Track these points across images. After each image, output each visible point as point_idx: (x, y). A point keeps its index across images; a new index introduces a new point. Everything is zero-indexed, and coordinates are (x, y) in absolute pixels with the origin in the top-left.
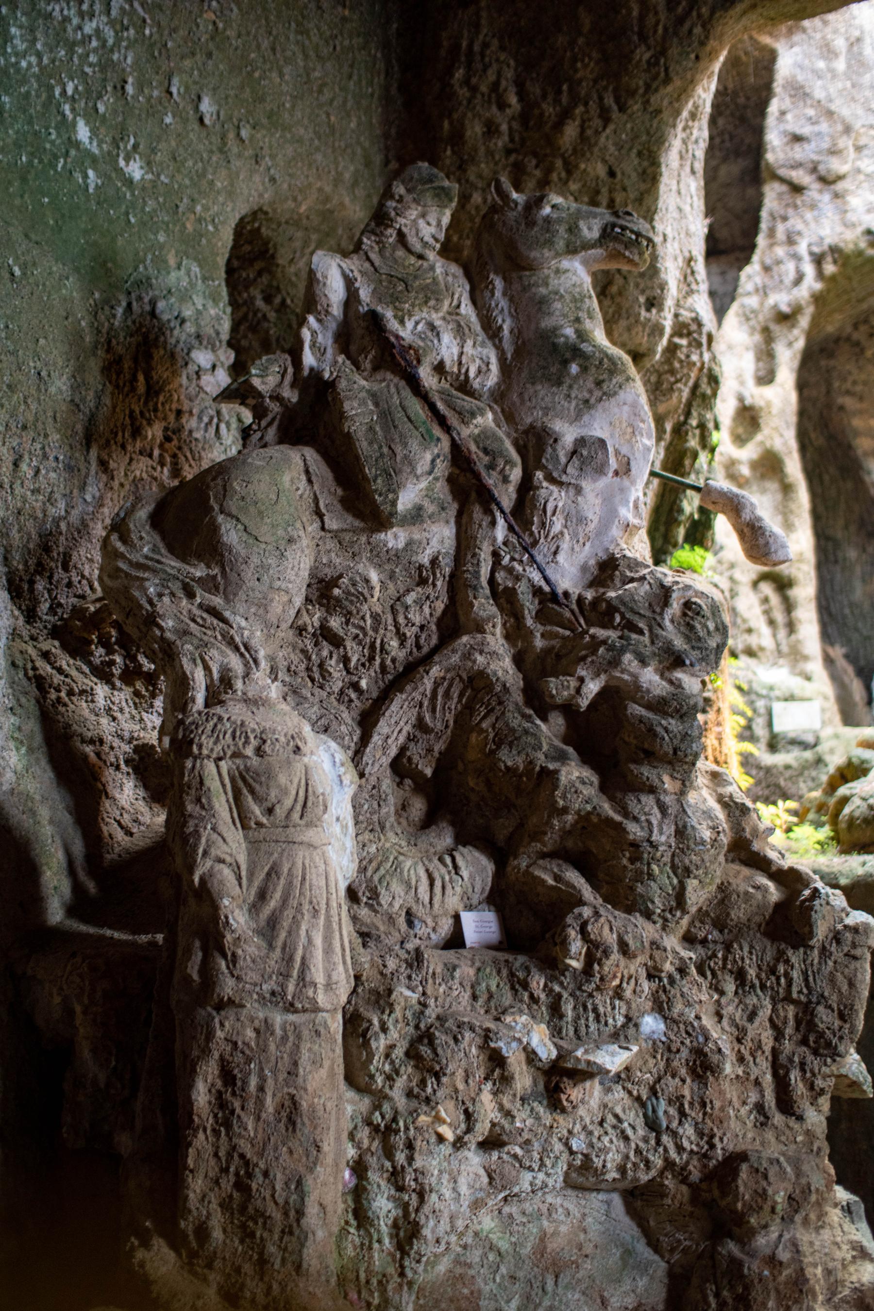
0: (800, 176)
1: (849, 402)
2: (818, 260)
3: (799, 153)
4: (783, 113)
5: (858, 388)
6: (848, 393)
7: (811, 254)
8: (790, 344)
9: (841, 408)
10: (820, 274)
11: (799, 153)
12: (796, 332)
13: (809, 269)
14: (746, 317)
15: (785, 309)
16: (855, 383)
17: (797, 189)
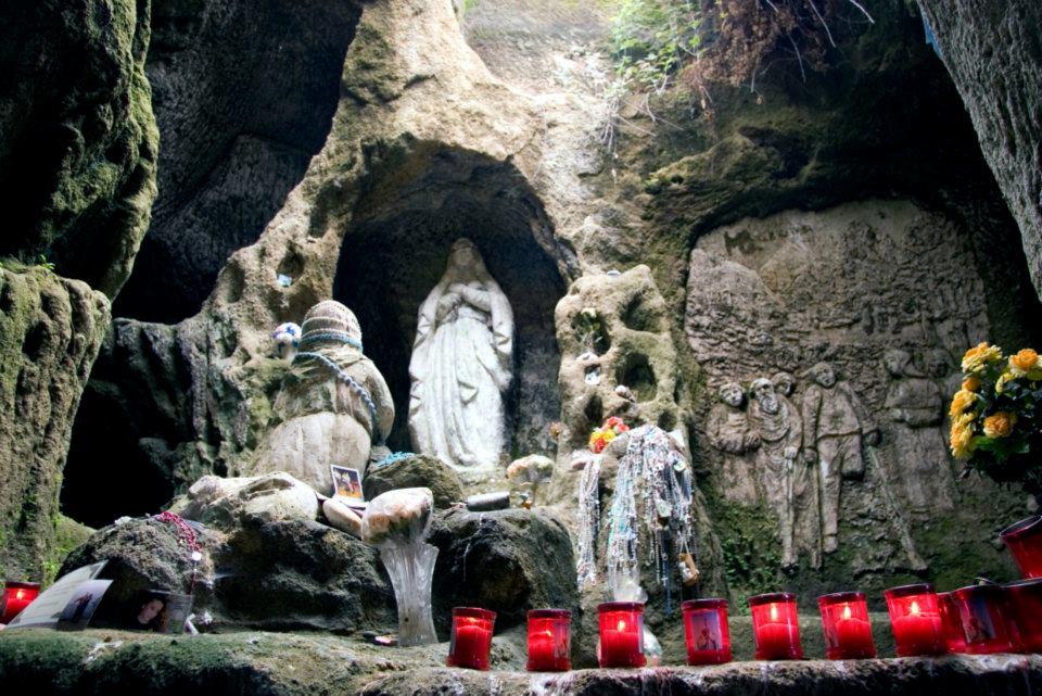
0: (366, 95)
1: (399, 288)
2: (367, 151)
3: (368, 76)
4: (359, 49)
5: (407, 278)
6: (399, 280)
7: (363, 147)
8: (340, 216)
9: (393, 291)
10: (368, 161)
11: (368, 76)
12: (345, 206)
13: (359, 157)
14: (308, 192)
15: (337, 183)
16: (404, 274)
17: (362, 103)
